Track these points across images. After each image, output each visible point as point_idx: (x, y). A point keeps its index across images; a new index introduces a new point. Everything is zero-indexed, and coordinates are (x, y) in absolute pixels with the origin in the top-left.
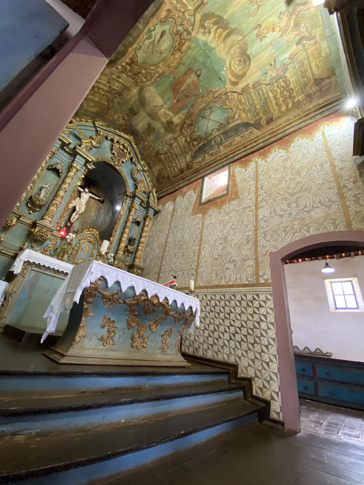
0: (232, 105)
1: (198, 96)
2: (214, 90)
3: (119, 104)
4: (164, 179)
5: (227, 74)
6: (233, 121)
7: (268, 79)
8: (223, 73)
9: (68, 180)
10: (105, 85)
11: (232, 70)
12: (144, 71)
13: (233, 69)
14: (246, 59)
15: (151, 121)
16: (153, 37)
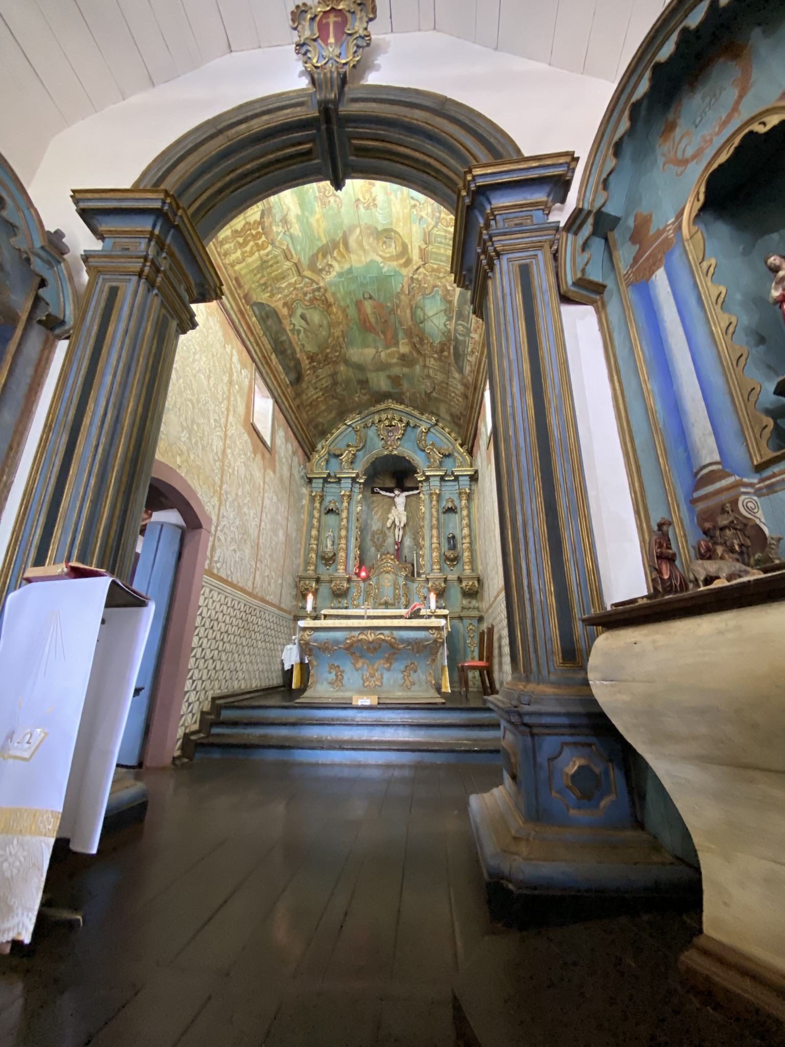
0: (432, 282)
1: (392, 310)
2: (399, 290)
5: (389, 266)
6: (451, 296)
7: (430, 220)
8: (385, 270)
9: (344, 515)
11: (390, 258)
12: (328, 351)
13: (388, 255)
14: (386, 235)
15: (387, 373)
16: (302, 329)
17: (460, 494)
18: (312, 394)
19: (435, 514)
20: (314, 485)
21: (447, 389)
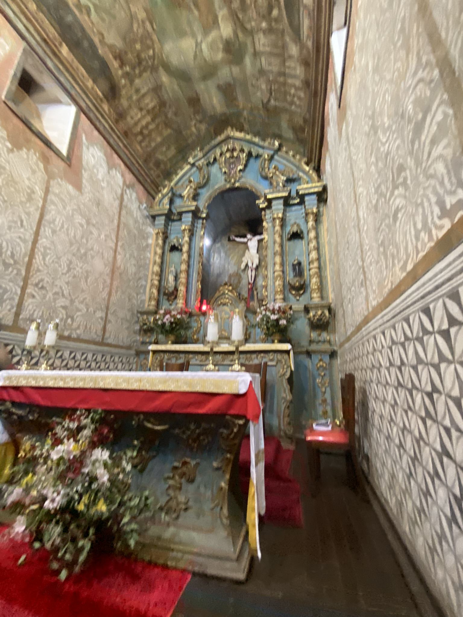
3: (176, 114)
4: (303, 131)
9: (185, 248)
10: (143, 117)
17: (307, 214)
18: (135, 116)
19: (278, 239)
20: (156, 222)
21: (284, 84)
